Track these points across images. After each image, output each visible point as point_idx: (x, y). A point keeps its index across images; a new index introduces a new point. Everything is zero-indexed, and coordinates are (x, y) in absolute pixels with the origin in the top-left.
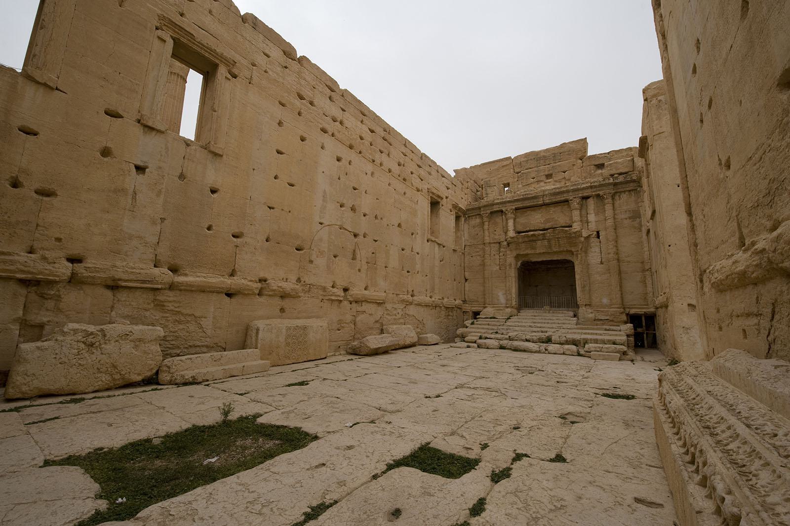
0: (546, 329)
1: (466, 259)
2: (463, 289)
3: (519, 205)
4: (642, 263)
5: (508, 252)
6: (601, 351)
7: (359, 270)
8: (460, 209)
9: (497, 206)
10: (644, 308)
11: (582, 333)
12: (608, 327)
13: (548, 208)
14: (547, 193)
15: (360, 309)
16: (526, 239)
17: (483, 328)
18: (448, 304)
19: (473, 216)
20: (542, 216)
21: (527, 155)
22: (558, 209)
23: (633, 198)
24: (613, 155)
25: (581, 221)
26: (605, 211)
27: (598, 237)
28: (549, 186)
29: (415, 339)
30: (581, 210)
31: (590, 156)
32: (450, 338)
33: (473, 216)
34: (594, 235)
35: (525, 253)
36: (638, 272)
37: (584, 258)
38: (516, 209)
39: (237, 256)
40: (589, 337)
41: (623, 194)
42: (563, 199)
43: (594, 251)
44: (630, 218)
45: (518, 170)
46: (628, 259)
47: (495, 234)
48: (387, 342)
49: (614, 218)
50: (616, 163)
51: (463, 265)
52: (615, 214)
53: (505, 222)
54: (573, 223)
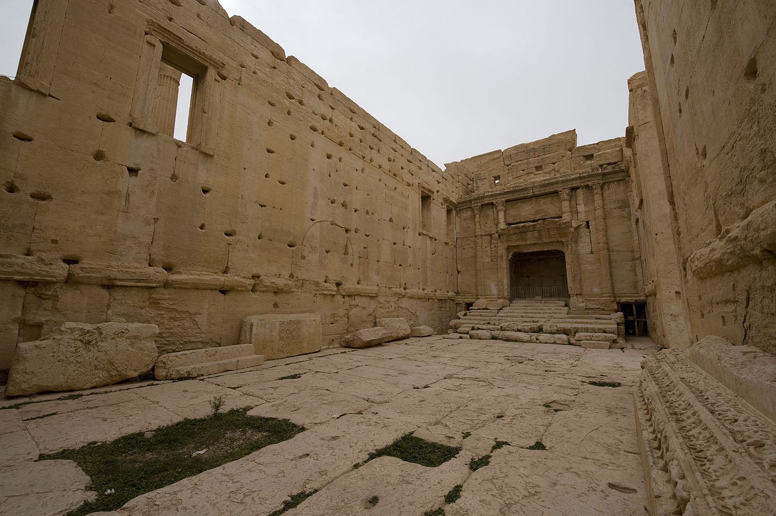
1: (458, 251)
2: (456, 283)
3: (510, 197)
4: (632, 251)
5: (499, 244)
6: (591, 340)
7: (352, 265)
8: (451, 202)
10: (634, 297)
11: (572, 323)
12: (598, 316)
15: (353, 303)
16: (517, 231)
17: (475, 319)
18: (441, 296)
19: (465, 209)
20: (532, 207)
21: (516, 148)
22: (547, 200)
23: (622, 188)
24: (602, 146)
25: (571, 212)
26: (594, 201)
27: (588, 227)
28: (539, 178)
29: (409, 331)
30: (570, 201)
32: (443, 329)
33: (465, 209)
34: (583, 225)
36: (627, 261)
37: (574, 248)
38: (507, 201)
39: (230, 253)
40: (580, 326)
41: (612, 184)
43: (583, 241)
44: (619, 208)
45: (507, 163)
46: (617, 248)
48: (380, 335)
50: (605, 153)
52: (604, 205)
53: (495, 214)
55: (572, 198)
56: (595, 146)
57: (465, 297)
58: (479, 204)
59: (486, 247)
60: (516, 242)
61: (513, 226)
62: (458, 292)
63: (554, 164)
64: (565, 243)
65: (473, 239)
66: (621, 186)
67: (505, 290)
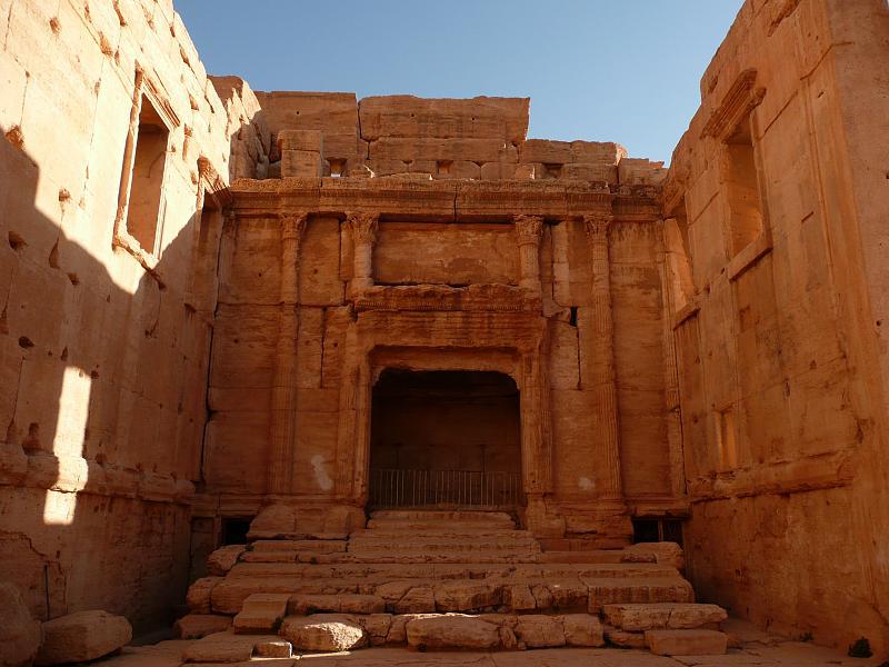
0: (477, 569)
3: (393, 208)
6: (666, 626)
9: (331, 200)
13: (462, 232)
14: (464, 189)
16: (410, 303)
20: (446, 249)
21: (396, 101)
23: (646, 242)
25: (540, 277)
26: (591, 261)
27: (573, 321)
31: (535, 143)
33: (253, 217)
35: (399, 343)
38: (383, 219)
40: (609, 584)
42: (501, 212)
44: (640, 285)
45: (368, 133)
46: (633, 382)
47: (316, 281)
49: (611, 283)
51: (206, 363)
52: (611, 272)
54: (521, 279)
55: (544, 243)
56: (568, 147)
57: (222, 498)
58: (303, 212)
59: (307, 343)
60: (398, 334)
61: (399, 287)
62: (203, 481)
63: (480, 164)
64: (525, 356)
65: (269, 313)
66: (645, 237)
67: (356, 476)
